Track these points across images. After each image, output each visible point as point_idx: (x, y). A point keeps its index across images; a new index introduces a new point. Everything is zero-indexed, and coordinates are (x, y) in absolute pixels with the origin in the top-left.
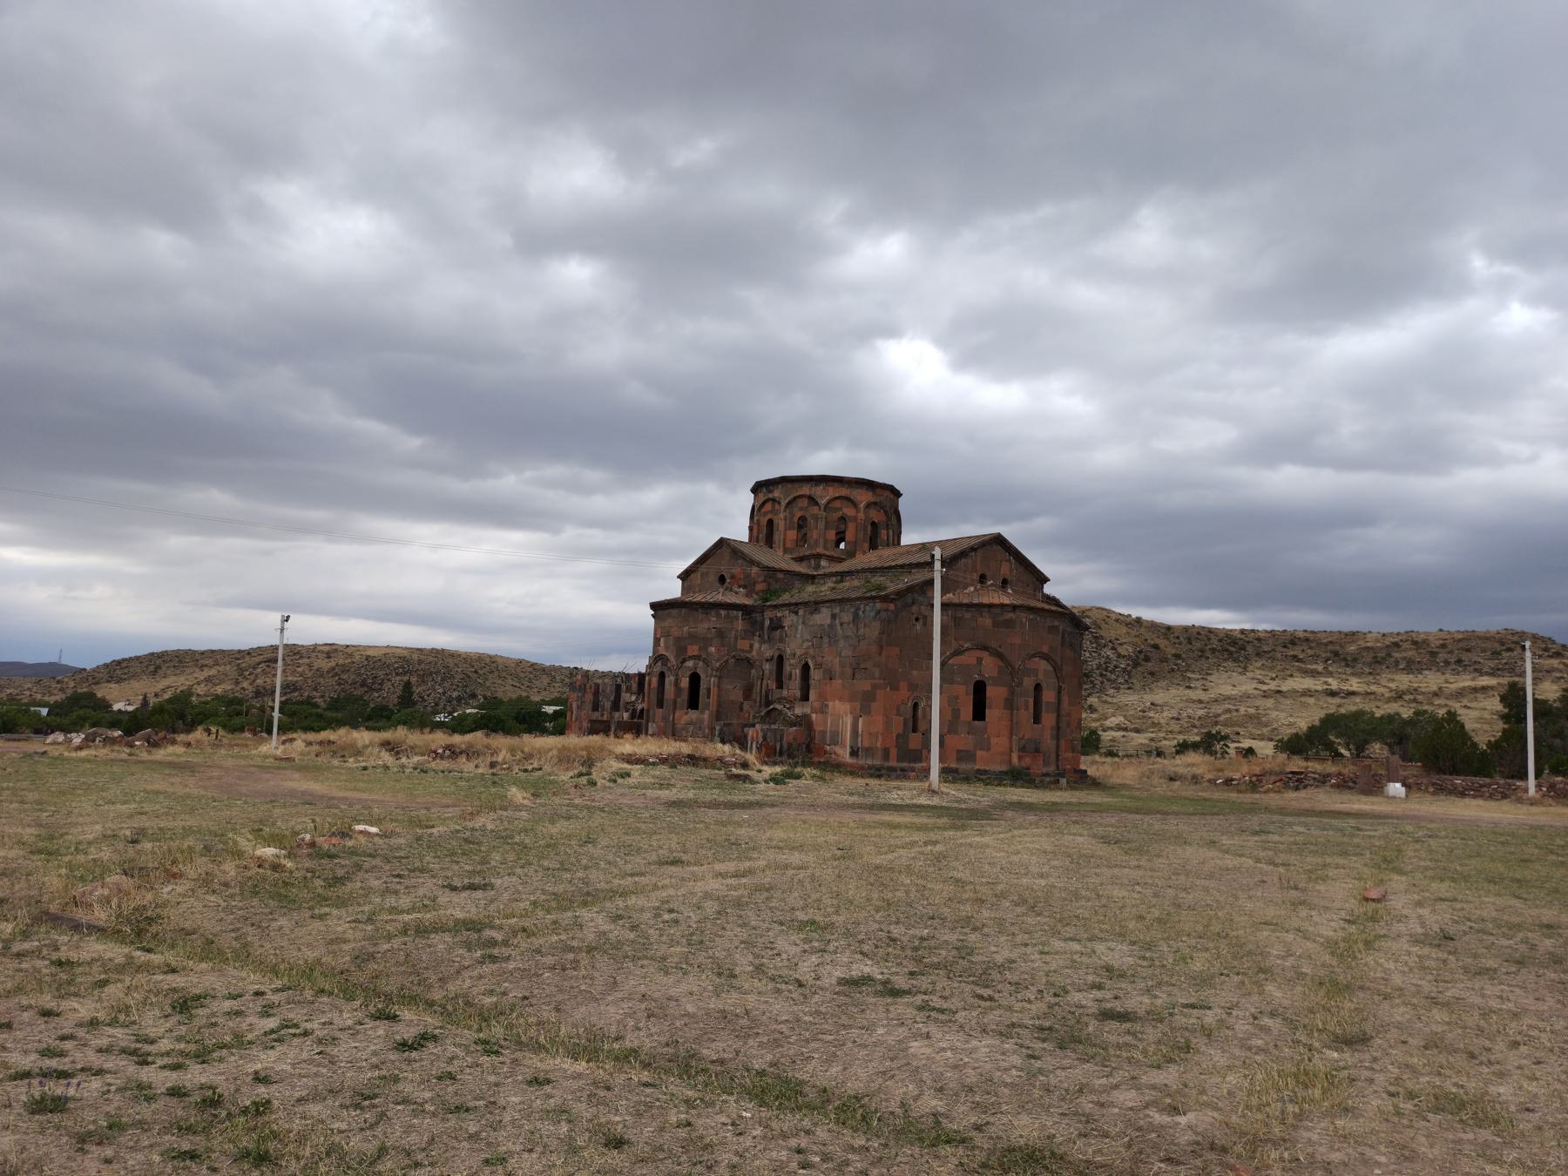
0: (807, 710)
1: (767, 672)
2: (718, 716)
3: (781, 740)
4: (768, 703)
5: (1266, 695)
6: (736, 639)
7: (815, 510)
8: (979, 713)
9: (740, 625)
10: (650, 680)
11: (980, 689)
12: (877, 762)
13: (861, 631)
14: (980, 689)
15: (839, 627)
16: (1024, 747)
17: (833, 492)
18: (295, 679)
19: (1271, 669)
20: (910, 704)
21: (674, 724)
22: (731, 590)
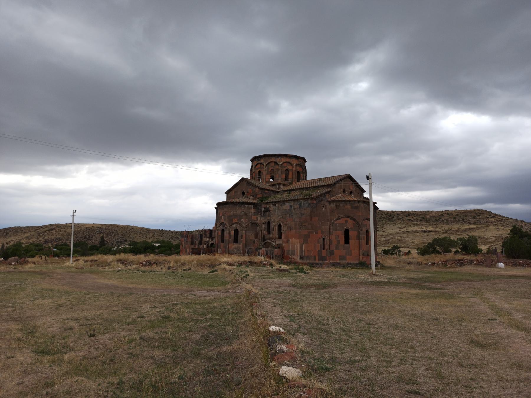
0: (281, 242)
1: (263, 228)
2: (246, 245)
3: (273, 254)
4: (264, 240)
5: (403, 233)
6: (251, 215)
7: (277, 167)
8: (347, 241)
9: (253, 210)
10: (218, 233)
11: (347, 232)
12: (311, 261)
13: (303, 212)
14: (347, 232)
15: (293, 210)
16: (364, 254)
17: (283, 160)
18: (60, 236)
19: (403, 224)
20: (322, 239)
21: (229, 249)
22: (247, 197)
